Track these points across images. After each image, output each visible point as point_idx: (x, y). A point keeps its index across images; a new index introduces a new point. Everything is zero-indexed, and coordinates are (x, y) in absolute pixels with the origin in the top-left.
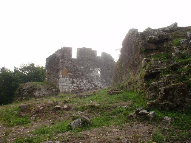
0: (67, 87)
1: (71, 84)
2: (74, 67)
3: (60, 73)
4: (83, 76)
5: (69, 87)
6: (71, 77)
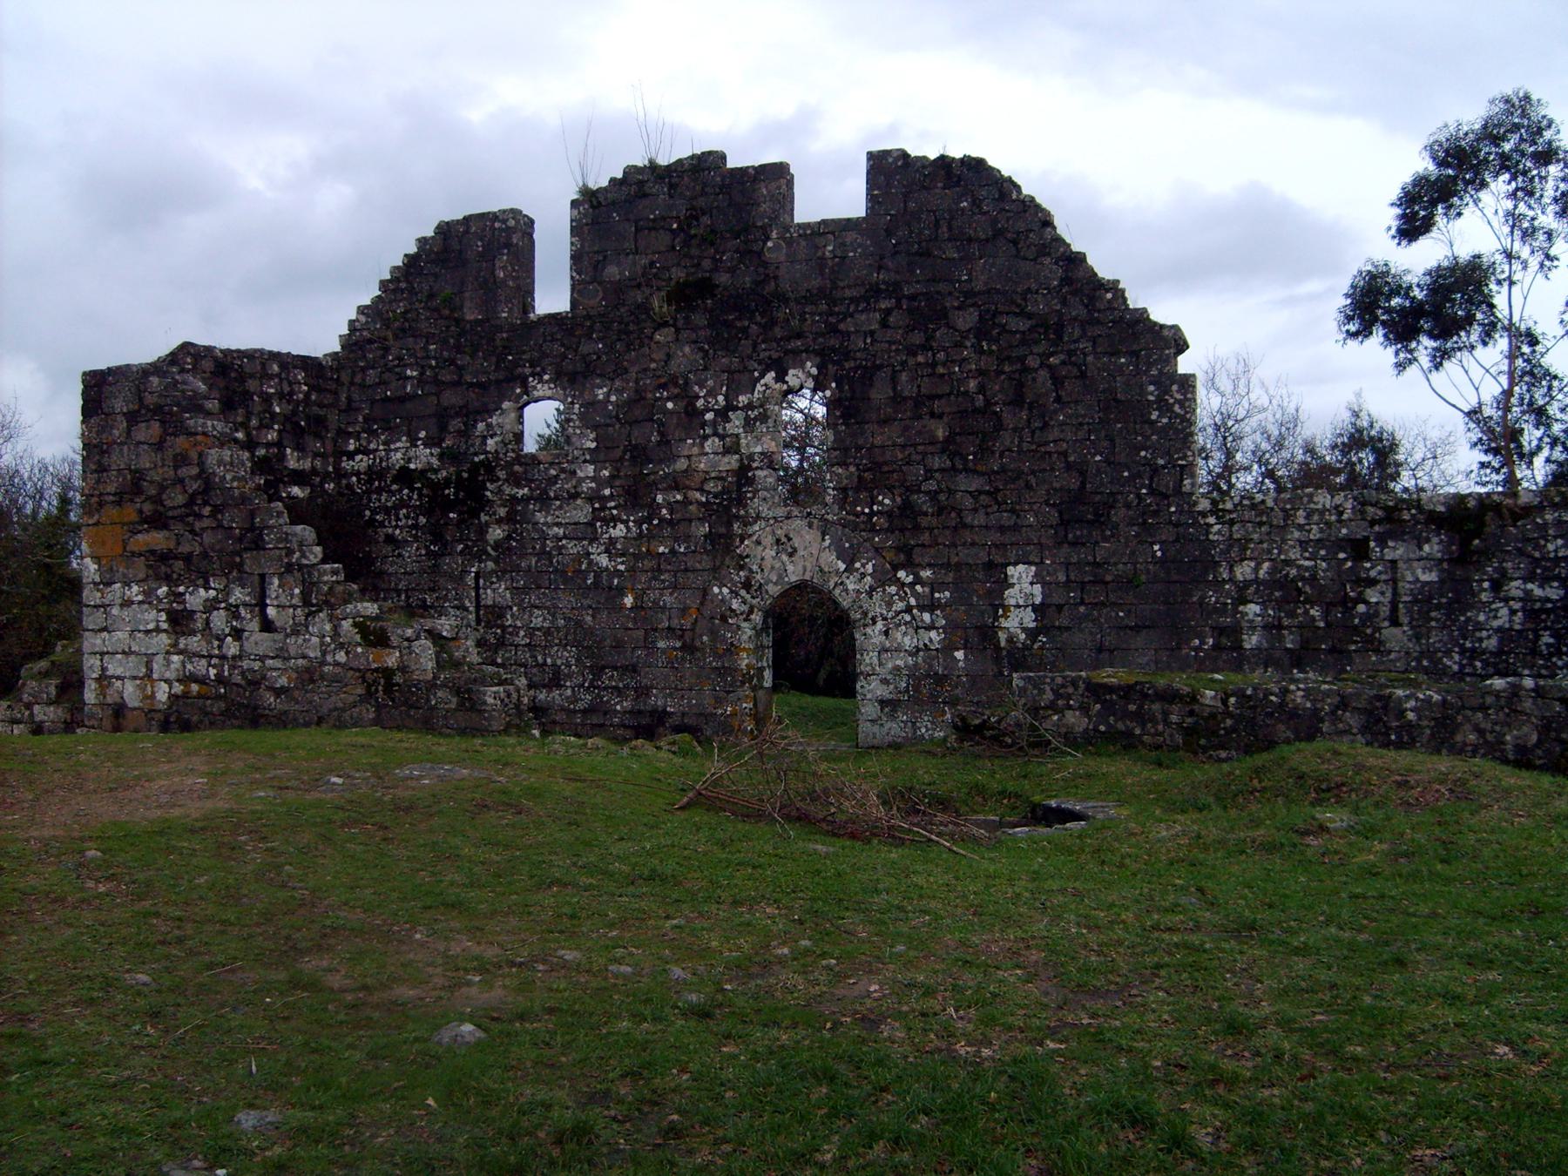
0: (134, 666)
1: (164, 640)
2: (184, 472)
4: (258, 545)
5: (150, 670)
6: (161, 566)
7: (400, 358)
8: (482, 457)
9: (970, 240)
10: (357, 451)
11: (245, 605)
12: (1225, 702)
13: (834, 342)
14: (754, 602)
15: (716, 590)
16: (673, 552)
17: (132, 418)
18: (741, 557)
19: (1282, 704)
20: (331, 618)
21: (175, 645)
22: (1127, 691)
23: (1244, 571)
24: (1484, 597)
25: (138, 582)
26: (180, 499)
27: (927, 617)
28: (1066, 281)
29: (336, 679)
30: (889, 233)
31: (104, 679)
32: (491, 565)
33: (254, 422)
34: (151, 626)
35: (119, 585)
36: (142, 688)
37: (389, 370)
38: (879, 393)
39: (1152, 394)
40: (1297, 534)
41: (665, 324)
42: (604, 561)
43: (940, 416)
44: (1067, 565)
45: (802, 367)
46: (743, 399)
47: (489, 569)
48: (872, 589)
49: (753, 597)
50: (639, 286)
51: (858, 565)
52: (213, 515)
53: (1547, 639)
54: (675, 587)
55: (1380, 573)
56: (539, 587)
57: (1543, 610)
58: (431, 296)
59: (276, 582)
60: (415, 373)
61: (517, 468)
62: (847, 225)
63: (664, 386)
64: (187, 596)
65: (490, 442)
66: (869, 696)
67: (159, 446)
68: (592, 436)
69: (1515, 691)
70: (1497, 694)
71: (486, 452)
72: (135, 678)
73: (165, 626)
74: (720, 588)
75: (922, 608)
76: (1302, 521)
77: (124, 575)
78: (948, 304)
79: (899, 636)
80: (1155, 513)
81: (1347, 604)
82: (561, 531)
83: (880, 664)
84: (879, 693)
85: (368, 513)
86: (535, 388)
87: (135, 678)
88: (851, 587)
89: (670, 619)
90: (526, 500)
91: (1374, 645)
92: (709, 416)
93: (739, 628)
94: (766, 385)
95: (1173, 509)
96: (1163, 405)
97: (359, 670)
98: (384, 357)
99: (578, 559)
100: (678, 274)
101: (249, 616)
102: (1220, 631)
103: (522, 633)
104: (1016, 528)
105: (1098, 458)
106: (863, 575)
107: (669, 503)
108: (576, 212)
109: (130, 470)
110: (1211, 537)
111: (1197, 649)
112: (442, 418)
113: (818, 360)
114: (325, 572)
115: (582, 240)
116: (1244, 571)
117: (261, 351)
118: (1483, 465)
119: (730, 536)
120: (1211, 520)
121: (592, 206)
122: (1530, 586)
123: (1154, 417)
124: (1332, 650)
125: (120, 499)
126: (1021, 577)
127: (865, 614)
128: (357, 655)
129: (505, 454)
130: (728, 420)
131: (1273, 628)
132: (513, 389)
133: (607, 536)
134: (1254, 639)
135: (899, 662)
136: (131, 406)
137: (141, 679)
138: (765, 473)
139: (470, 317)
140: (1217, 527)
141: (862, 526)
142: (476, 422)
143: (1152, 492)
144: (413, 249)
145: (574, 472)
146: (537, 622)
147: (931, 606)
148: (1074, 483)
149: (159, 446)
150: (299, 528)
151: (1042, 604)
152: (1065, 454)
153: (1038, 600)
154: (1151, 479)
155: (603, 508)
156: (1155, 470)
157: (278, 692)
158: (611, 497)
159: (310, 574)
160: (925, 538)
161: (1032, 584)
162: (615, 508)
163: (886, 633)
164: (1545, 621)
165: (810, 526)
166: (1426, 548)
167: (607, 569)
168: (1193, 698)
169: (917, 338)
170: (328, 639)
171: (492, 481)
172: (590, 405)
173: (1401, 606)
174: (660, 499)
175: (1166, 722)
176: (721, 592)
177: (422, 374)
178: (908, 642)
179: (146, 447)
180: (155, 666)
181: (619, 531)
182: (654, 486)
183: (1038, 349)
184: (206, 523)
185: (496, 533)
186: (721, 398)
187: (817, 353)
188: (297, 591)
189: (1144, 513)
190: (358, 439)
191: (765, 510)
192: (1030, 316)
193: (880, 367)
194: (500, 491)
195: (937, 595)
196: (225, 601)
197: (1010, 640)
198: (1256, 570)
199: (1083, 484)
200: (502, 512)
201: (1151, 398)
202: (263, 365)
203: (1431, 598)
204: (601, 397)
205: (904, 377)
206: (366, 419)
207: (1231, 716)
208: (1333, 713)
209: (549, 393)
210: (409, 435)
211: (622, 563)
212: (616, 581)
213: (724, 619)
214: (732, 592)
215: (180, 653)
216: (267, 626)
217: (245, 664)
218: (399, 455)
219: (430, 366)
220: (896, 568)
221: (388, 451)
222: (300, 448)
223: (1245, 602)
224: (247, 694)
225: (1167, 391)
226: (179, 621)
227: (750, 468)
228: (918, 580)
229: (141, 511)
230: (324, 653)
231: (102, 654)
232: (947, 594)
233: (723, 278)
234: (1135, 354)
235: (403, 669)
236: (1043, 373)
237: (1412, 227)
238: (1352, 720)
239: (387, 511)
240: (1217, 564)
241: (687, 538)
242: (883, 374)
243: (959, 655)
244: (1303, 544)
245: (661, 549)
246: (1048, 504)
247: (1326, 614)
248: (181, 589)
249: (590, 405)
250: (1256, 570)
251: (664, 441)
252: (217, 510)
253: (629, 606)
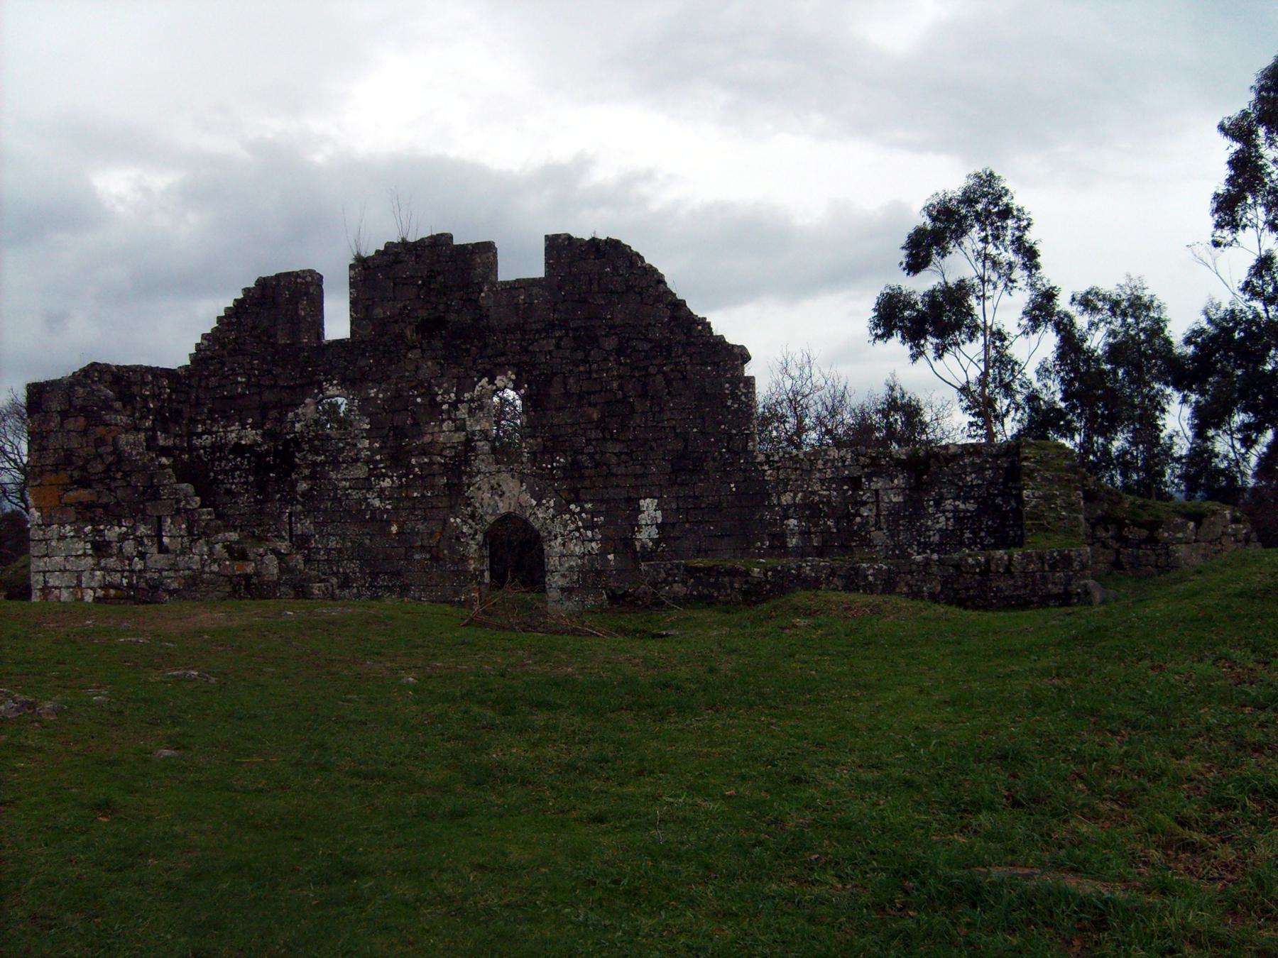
1: (90, 561)
2: (102, 450)
4: (156, 496)
5: (80, 582)
6: (86, 512)
7: (233, 369)
8: (292, 435)
9: (612, 292)
10: (204, 433)
11: (148, 536)
12: (765, 575)
13: (526, 358)
14: (477, 527)
15: (452, 520)
16: (423, 496)
17: (64, 415)
18: (468, 498)
19: (799, 575)
20: (208, 543)
22: (709, 571)
23: (786, 499)
24: (931, 511)
25: (70, 524)
26: (100, 468)
27: (589, 533)
28: (673, 318)
29: (210, 582)
30: (560, 288)
31: (46, 589)
32: (299, 507)
33: (137, 415)
34: (80, 552)
36: (74, 594)
37: (227, 378)
38: (556, 390)
39: (727, 389)
40: (818, 475)
41: (415, 347)
42: (377, 503)
43: (595, 405)
44: (678, 498)
45: (506, 374)
47: (298, 510)
48: (554, 516)
49: (477, 524)
50: (396, 322)
51: (544, 501)
52: (124, 477)
53: (968, 535)
54: (425, 519)
55: (869, 497)
56: (333, 522)
57: (965, 517)
58: (254, 328)
60: (244, 380)
61: (316, 442)
62: (534, 282)
63: (415, 388)
65: (297, 425)
66: (554, 586)
68: (367, 421)
69: (927, 561)
70: (918, 564)
71: (294, 432)
72: (68, 587)
73: (90, 552)
74: (455, 519)
75: (586, 528)
76: (821, 467)
77: (60, 519)
78: (599, 334)
79: (572, 546)
80: (731, 464)
81: (850, 517)
82: (348, 484)
83: (561, 565)
84: (560, 583)
85: (212, 474)
86: (327, 389)
87: (68, 587)
88: (540, 516)
89: (422, 539)
90: (323, 464)
91: (866, 542)
92: (445, 407)
93: (468, 544)
94: (482, 386)
95: (742, 461)
96: (735, 398)
97: (227, 576)
98: (221, 369)
99: (359, 502)
100: (423, 314)
101: (150, 543)
102: (773, 536)
103: (322, 552)
104: (644, 475)
105: (695, 430)
106: (548, 508)
107: (420, 464)
108: (353, 272)
109: (63, 448)
110: (766, 478)
111: (759, 549)
112: (263, 411)
113: (516, 370)
114: (203, 514)
115: (358, 291)
116: (786, 499)
117: (141, 367)
118: (971, 424)
119: (460, 485)
120: (766, 467)
121: (364, 269)
122: (957, 503)
123: (729, 404)
124: (842, 546)
125: (56, 468)
126: (648, 505)
127: (550, 533)
128: (226, 566)
129: (308, 433)
130: (457, 409)
131: (805, 534)
132: (313, 389)
133: (378, 486)
134: (794, 540)
135: (573, 563)
136: (63, 407)
138: (483, 443)
139: (282, 342)
140: (769, 472)
141: (547, 476)
142: (287, 412)
143: (729, 450)
144: (240, 296)
145: (355, 445)
146: (333, 543)
147: (592, 527)
149: (84, 433)
150: (184, 485)
151: (662, 523)
152: (674, 428)
153: (660, 521)
154: (728, 443)
155: (376, 468)
156: (731, 437)
158: (381, 461)
159: (193, 515)
160: (587, 483)
161: (655, 510)
162: (383, 468)
163: (564, 545)
164: (966, 524)
165: (513, 477)
166: (896, 481)
167: (379, 508)
168: (747, 573)
169: (580, 355)
170: (206, 557)
171: (299, 452)
172: (366, 400)
173: (882, 517)
174: (413, 461)
175: (733, 588)
176: (455, 522)
177: (249, 380)
178: (578, 550)
179: (74, 434)
180: (84, 579)
181: (386, 483)
182: (409, 454)
183: (655, 362)
184: (119, 483)
185: (303, 486)
187: (514, 365)
188: (184, 526)
189: (724, 464)
190: (204, 424)
191: (483, 468)
192: (650, 341)
193: (556, 374)
194: (305, 458)
195: (595, 519)
197: (643, 546)
198: (794, 498)
199: (686, 447)
200: (307, 472)
201: (727, 392)
202: (142, 376)
203: (898, 513)
204: (373, 395)
205: (571, 380)
206: (210, 411)
207: (768, 582)
208: (827, 578)
209: (337, 393)
210: (240, 421)
211: (389, 504)
212: (385, 516)
213: (458, 539)
214: (462, 521)
215: (102, 569)
216: (163, 549)
217: (148, 575)
218: (234, 435)
219: (255, 375)
220: (569, 503)
221: (225, 432)
222: (165, 431)
223: (788, 518)
224: (150, 594)
225: (738, 388)
226: (101, 548)
227: (473, 441)
228: (583, 510)
229: (71, 476)
230: (203, 566)
231: (45, 572)
232: (602, 518)
233: (452, 317)
234: (716, 364)
235: (258, 574)
236: (659, 378)
237: (916, 263)
238: (838, 582)
239: (226, 472)
240: (770, 495)
241: (432, 487)
242: (558, 379)
243: (611, 557)
244: (822, 481)
245: (415, 494)
246: (664, 459)
247: (837, 523)
248: (102, 527)
249: (366, 400)
250: (794, 498)
251: (416, 423)
252: (126, 475)
253: (394, 532)
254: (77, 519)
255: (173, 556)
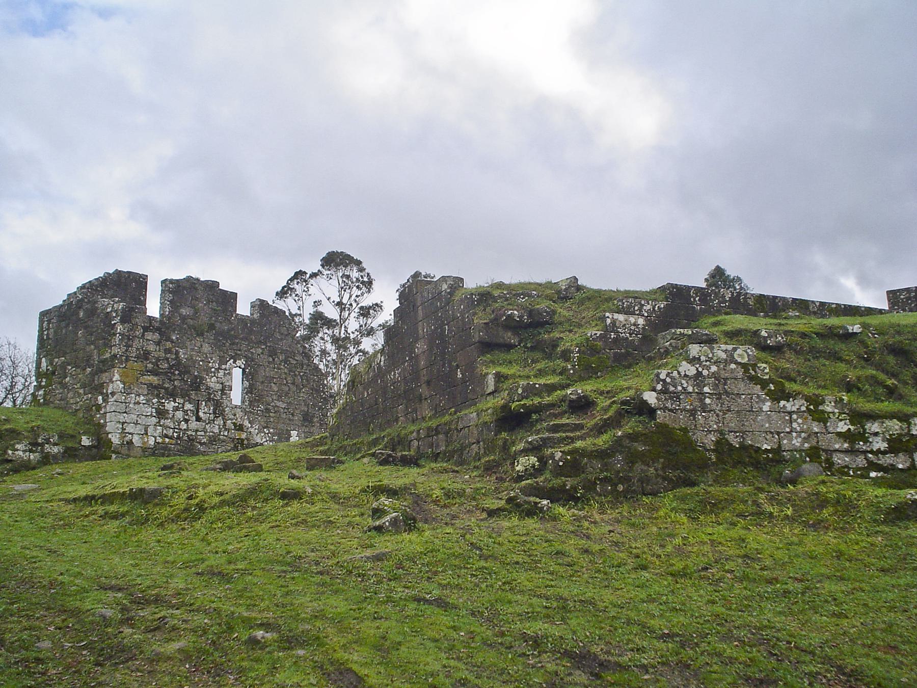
0: (139, 429)
1: (154, 420)
3: (117, 377)
5: (146, 431)
20: (223, 419)
21: (159, 422)
25: (143, 395)
34: (148, 414)
35: (133, 395)
46: (224, 367)
48: (258, 433)
59: (204, 403)
64: (166, 404)
67: (158, 343)
72: (139, 434)
73: (155, 414)
75: (270, 441)
77: (137, 392)
87: (139, 434)
92: (213, 370)
106: (255, 429)
128: (232, 433)
137: (142, 435)
148: (306, 409)
149: (158, 343)
157: (201, 444)
186: (217, 365)
188: (212, 408)
196: (183, 408)
215: (160, 426)
216: (198, 419)
217: (190, 433)
220: (264, 428)
226: (161, 414)
230: (220, 432)
231: (123, 423)
248: (163, 401)
254: (148, 394)
255: (204, 424)
